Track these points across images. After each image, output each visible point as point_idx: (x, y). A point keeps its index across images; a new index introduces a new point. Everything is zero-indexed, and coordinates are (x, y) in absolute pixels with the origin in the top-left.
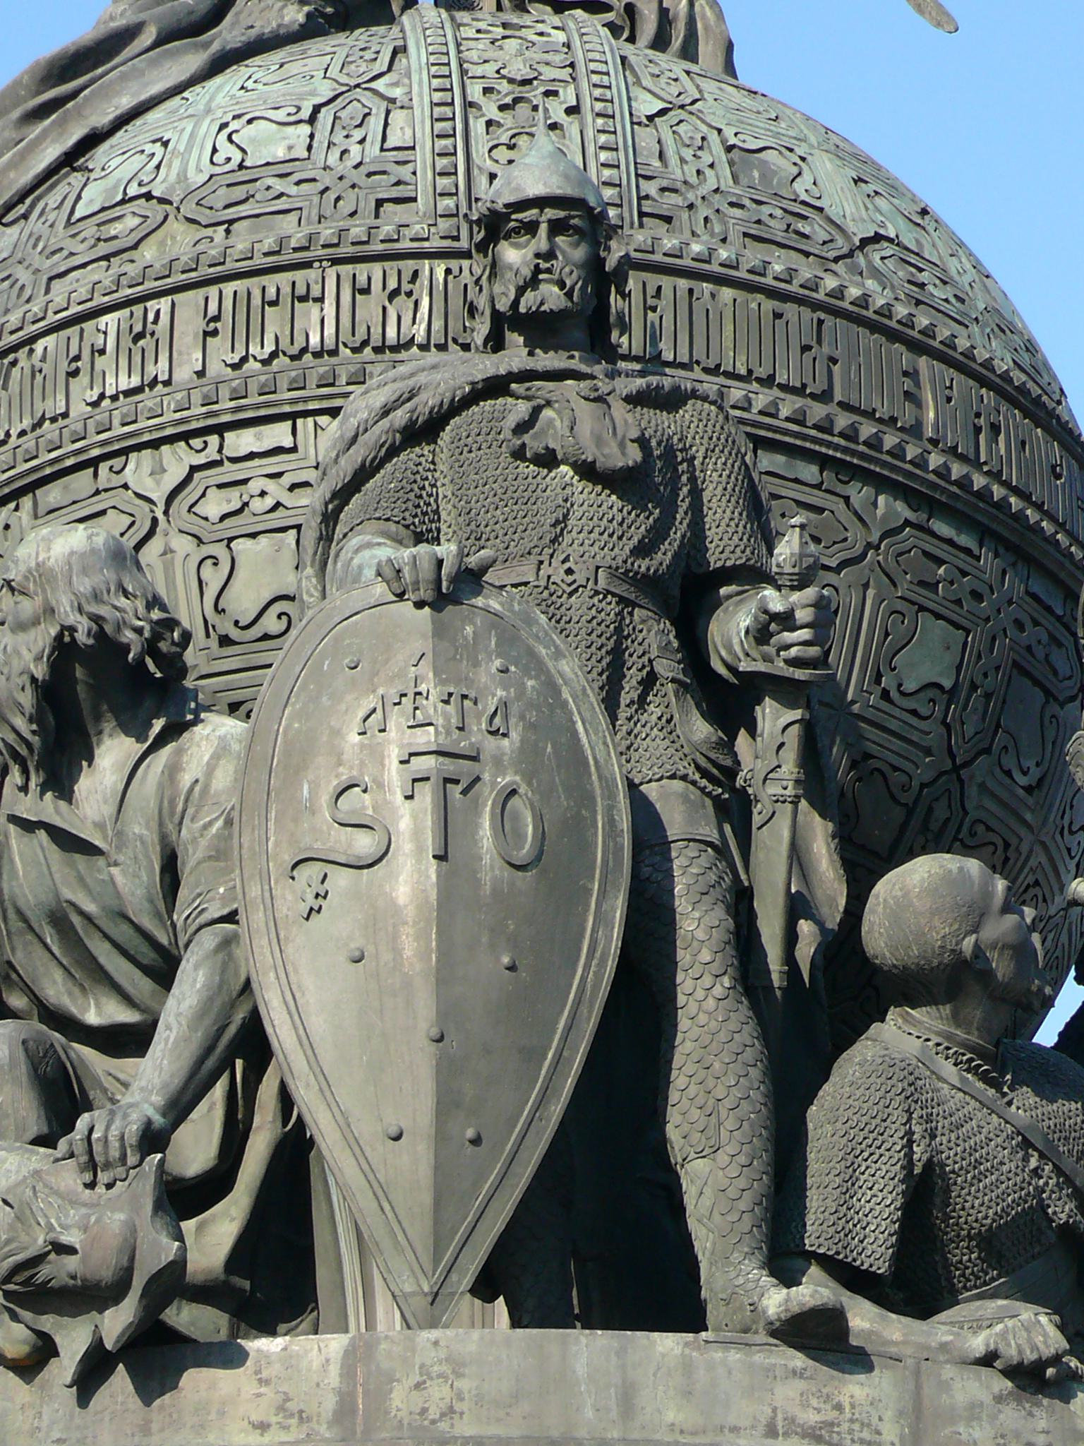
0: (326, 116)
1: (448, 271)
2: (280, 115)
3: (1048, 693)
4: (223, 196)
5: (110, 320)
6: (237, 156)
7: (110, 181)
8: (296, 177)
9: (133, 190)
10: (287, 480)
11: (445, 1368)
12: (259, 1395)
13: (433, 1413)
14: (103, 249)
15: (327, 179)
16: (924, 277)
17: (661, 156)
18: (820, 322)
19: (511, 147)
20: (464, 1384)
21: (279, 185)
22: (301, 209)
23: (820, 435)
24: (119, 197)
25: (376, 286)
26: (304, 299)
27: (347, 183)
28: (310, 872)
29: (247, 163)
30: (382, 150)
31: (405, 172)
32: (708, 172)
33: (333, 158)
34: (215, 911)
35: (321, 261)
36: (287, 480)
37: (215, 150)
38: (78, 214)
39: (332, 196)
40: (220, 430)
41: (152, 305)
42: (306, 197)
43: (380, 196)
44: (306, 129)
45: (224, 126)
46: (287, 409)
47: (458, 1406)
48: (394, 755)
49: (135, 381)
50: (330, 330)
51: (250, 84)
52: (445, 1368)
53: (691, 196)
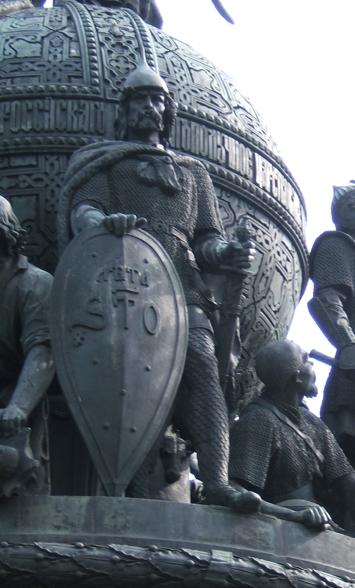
0: (46, 42)
1: (96, 106)
2: (29, 39)
3: (284, 278)
4: (8, 67)
6: (14, 53)
8: (37, 64)
10: (34, 177)
11: (123, 511)
12: (57, 516)
13: (119, 527)
15: (49, 66)
16: (254, 123)
17: (168, 70)
18: (223, 138)
19: (117, 61)
20: (130, 518)
21: (31, 66)
22: (39, 76)
23: (220, 178)
25: (69, 109)
26: (41, 111)
27: (57, 68)
28: (79, 331)
29: (18, 56)
30: (70, 57)
31: (78, 66)
32: (184, 77)
33: (51, 58)
34: (39, 339)
35: (48, 97)
36: (34, 177)
37: (4, 49)
39: (51, 72)
40: (9, 156)
42: (42, 72)
43: (69, 74)
44: (39, 46)
46: (35, 151)
47: (128, 525)
48: (110, 289)
50: (52, 123)
51: (14, 25)
52: (123, 511)
53: (178, 86)
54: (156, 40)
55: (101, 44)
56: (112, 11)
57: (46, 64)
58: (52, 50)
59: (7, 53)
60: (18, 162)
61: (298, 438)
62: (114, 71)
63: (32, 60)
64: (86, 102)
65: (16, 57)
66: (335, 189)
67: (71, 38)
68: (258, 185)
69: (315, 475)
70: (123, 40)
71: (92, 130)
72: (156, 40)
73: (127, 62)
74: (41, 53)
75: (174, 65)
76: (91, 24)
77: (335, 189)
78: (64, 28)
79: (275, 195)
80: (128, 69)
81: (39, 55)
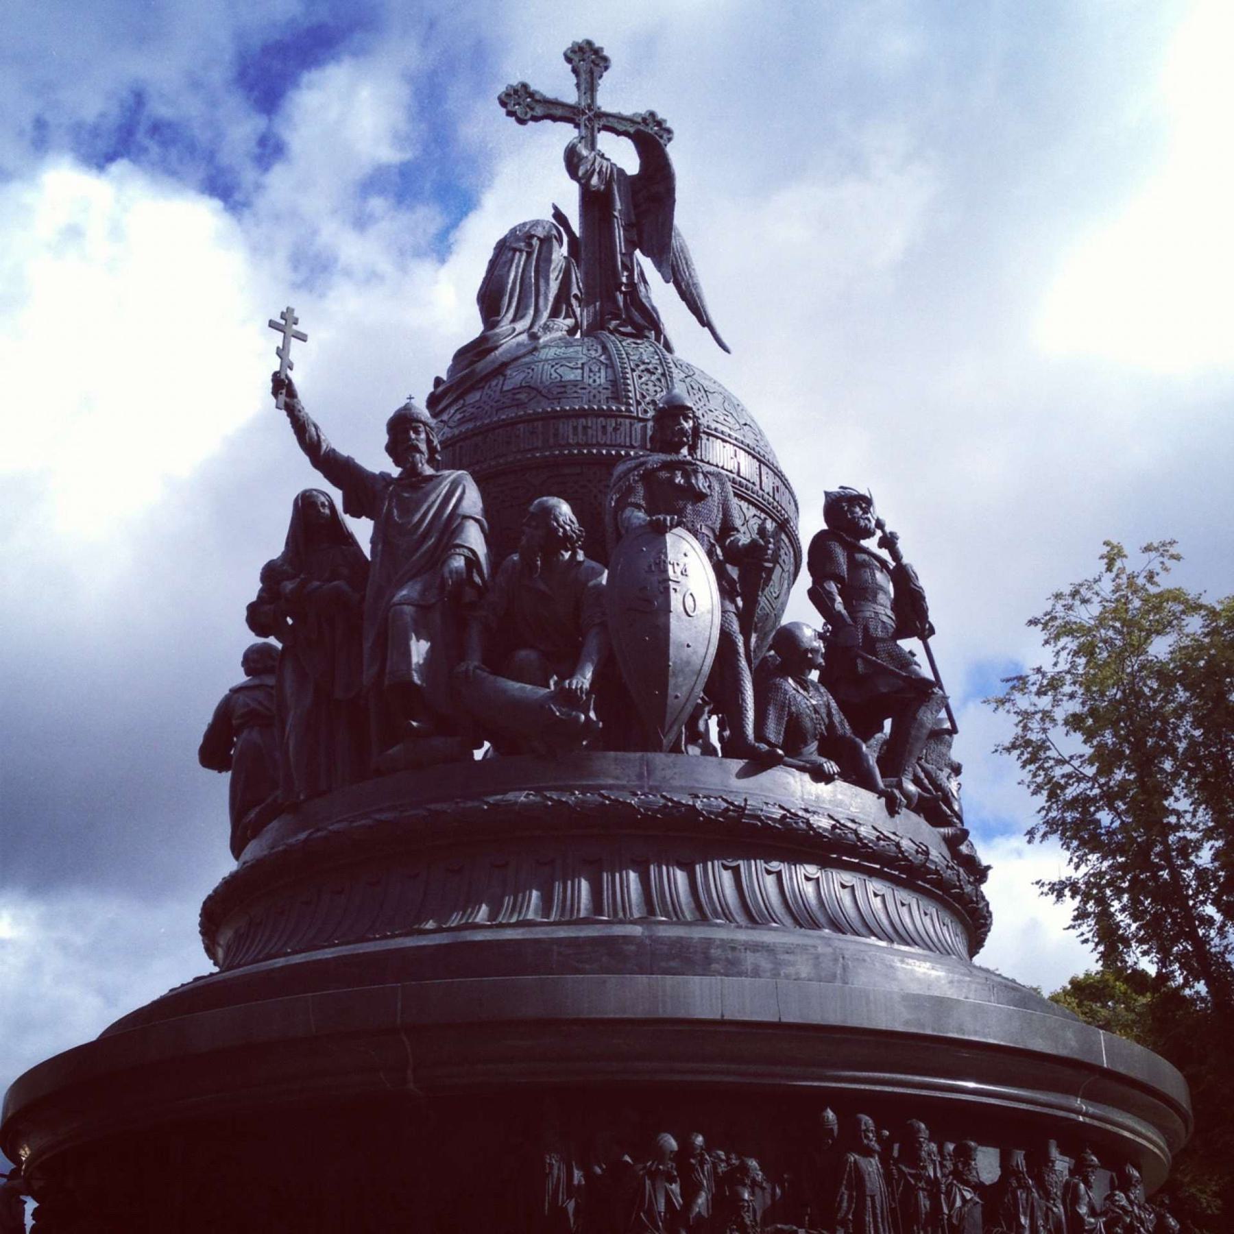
0: (586, 369)
2: (571, 365)
3: (783, 570)
4: (556, 391)
5: (521, 426)
6: (559, 377)
7: (513, 381)
9: (523, 384)
14: (515, 403)
16: (758, 438)
17: (688, 392)
18: (735, 451)
19: (647, 384)
21: (574, 389)
24: (519, 385)
33: (591, 381)
38: (505, 388)
39: (592, 394)
41: (536, 424)
42: (584, 394)
45: (553, 366)
49: (530, 447)
54: (676, 367)
55: (633, 370)
56: (639, 341)
57: (587, 386)
58: (592, 375)
59: (553, 377)
60: (567, 471)
61: (809, 704)
62: (645, 393)
63: (575, 383)
64: (622, 420)
65: (561, 381)
66: (827, 494)
67: (606, 365)
68: (763, 491)
69: (822, 734)
70: (650, 366)
71: (628, 444)
72: (676, 367)
73: (655, 386)
74: (583, 377)
75: (693, 388)
76: (623, 352)
77: (827, 494)
78: (601, 356)
79: (777, 499)
80: (656, 391)
81: (579, 378)
